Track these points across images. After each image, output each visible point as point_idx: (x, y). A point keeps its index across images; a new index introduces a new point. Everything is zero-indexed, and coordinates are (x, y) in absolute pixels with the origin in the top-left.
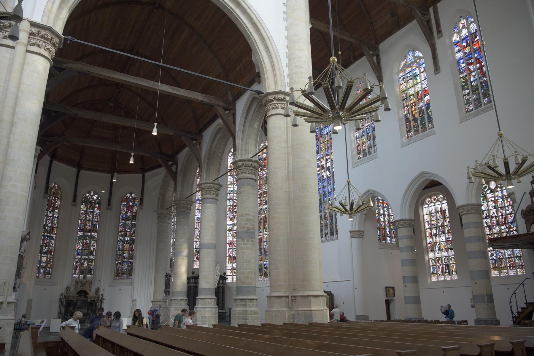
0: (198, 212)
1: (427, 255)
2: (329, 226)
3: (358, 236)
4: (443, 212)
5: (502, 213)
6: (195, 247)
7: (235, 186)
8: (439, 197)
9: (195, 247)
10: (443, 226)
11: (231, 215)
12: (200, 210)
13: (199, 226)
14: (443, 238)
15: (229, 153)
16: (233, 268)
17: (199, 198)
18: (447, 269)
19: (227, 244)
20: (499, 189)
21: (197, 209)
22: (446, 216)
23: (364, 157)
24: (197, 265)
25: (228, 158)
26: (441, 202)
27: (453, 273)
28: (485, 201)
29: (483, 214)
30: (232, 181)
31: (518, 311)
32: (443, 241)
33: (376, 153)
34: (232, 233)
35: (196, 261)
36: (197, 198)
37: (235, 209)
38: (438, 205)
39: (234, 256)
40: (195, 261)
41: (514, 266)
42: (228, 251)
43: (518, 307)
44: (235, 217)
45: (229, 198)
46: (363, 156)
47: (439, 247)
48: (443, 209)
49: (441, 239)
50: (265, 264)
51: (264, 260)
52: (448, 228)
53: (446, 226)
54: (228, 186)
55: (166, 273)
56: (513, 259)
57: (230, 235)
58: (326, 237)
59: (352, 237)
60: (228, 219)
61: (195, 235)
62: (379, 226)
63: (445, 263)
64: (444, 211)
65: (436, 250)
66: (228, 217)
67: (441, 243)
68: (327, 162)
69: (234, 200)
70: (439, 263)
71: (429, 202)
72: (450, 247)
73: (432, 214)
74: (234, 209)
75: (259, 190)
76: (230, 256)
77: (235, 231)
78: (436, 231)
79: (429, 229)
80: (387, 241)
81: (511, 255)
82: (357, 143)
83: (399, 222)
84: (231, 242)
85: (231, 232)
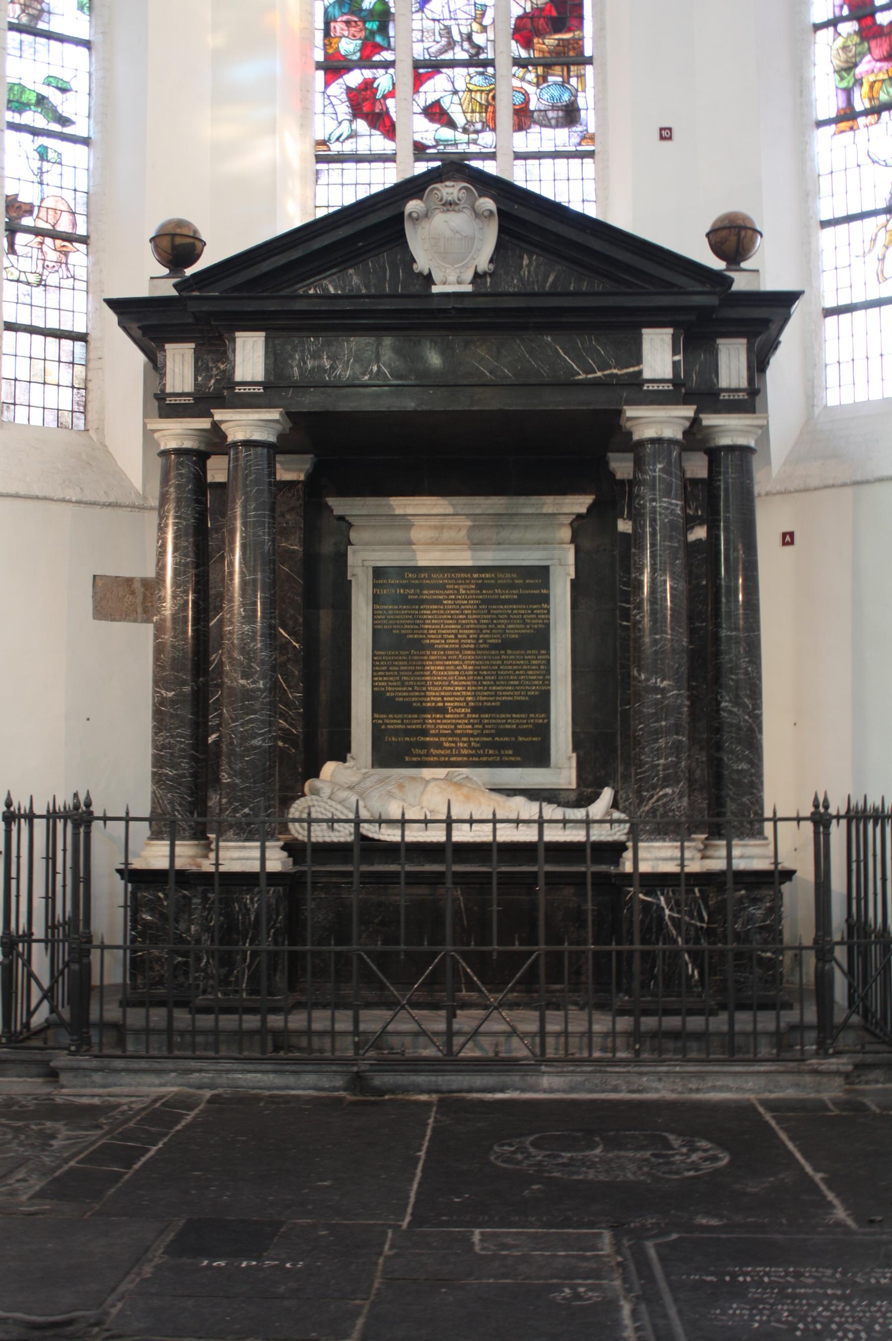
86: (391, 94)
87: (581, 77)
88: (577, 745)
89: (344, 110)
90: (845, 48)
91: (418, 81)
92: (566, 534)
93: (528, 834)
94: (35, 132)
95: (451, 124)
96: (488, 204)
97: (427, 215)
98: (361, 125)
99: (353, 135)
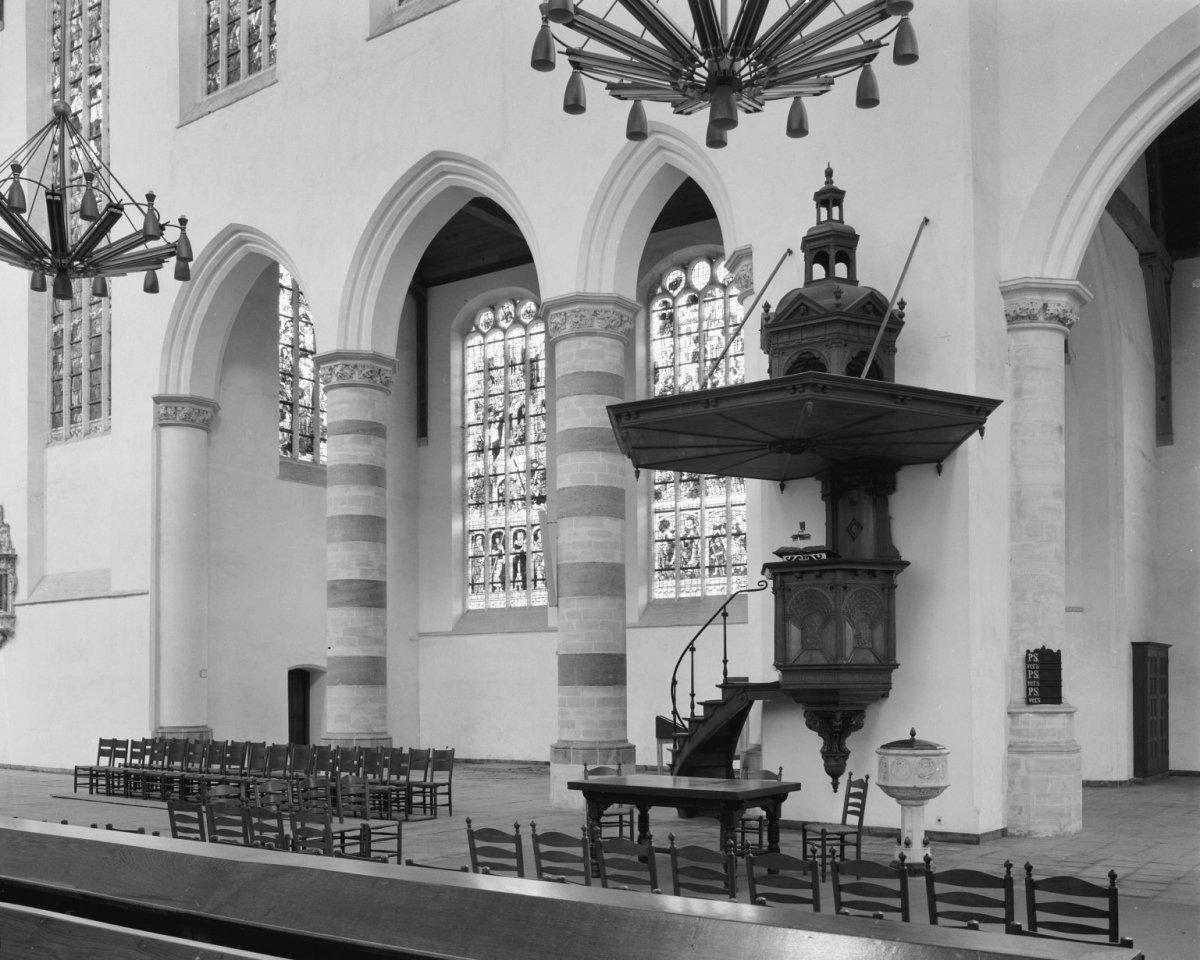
1: (461, 517)
2: (85, 378)
3: (188, 422)
4: (529, 365)
5: (714, 381)
8: (522, 311)
10: (524, 417)
14: (520, 460)
18: (519, 569)
20: (718, 292)
22: (538, 380)
23: (229, 81)
26: (526, 326)
27: (535, 585)
28: (670, 334)
29: (656, 381)
31: (693, 714)
32: (518, 472)
33: (271, 68)
38: (516, 340)
41: (725, 566)
43: (697, 699)
46: (229, 79)
47: (501, 491)
48: (533, 356)
49: (510, 462)
52: (539, 424)
53: (534, 416)
56: (724, 540)
58: (72, 422)
59: (165, 422)
62: (289, 395)
63: (513, 550)
64: (532, 361)
65: (491, 503)
67: (511, 479)
68: (94, 101)
70: (497, 549)
71: (487, 324)
72: (537, 494)
73: (494, 373)
78: (500, 434)
79: (477, 425)
80: (318, 455)
81: (719, 528)
82: (209, 18)
83: (332, 364)
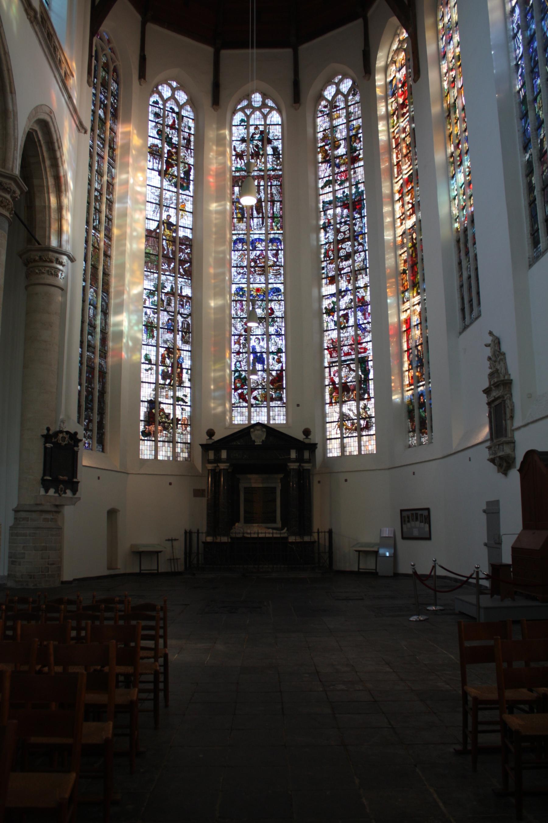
0: (239, 273)
6: (233, 368)
7: (337, 187)
9: (233, 368)
11: (330, 269)
12: (245, 267)
13: (242, 310)
15: (320, 104)
16: (343, 417)
17: (241, 236)
19: (326, 352)
21: (237, 267)
24: (242, 414)
25: (315, 118)
30: (329, 176)
34: (335, 318)
35: (238, 405)
36: (235, 237)
37: (342, 248)
39: (343, 381)
40: (236, 405)
42: (327, 370)
44: (342, 272)
45: (324, 223)
50: (421, 394)
51: (419, 382)
54: (321, 192)
55: (48, 429)
57: (332, 325)
60: (324, 281)
61: (234, 335)
66: (324, 276)
69: (338, 226)
74: (339, 250)
75: (397, 178)
76: (333, 382)
77: (344, 310)
84: (334, 344)
85: (333, 316)
86: (247, 394)
87: (283, 392)
88: (281, 519)
89: (237, 397)
90: (331, 390)
91: (252, 392)
92: (279, 481)
93: (271, 535)
94: (181, 405)
95: (258, 400)
96: (264, 430)
97: (254, 431)
98: (241, 400)
99: (240, 402)
